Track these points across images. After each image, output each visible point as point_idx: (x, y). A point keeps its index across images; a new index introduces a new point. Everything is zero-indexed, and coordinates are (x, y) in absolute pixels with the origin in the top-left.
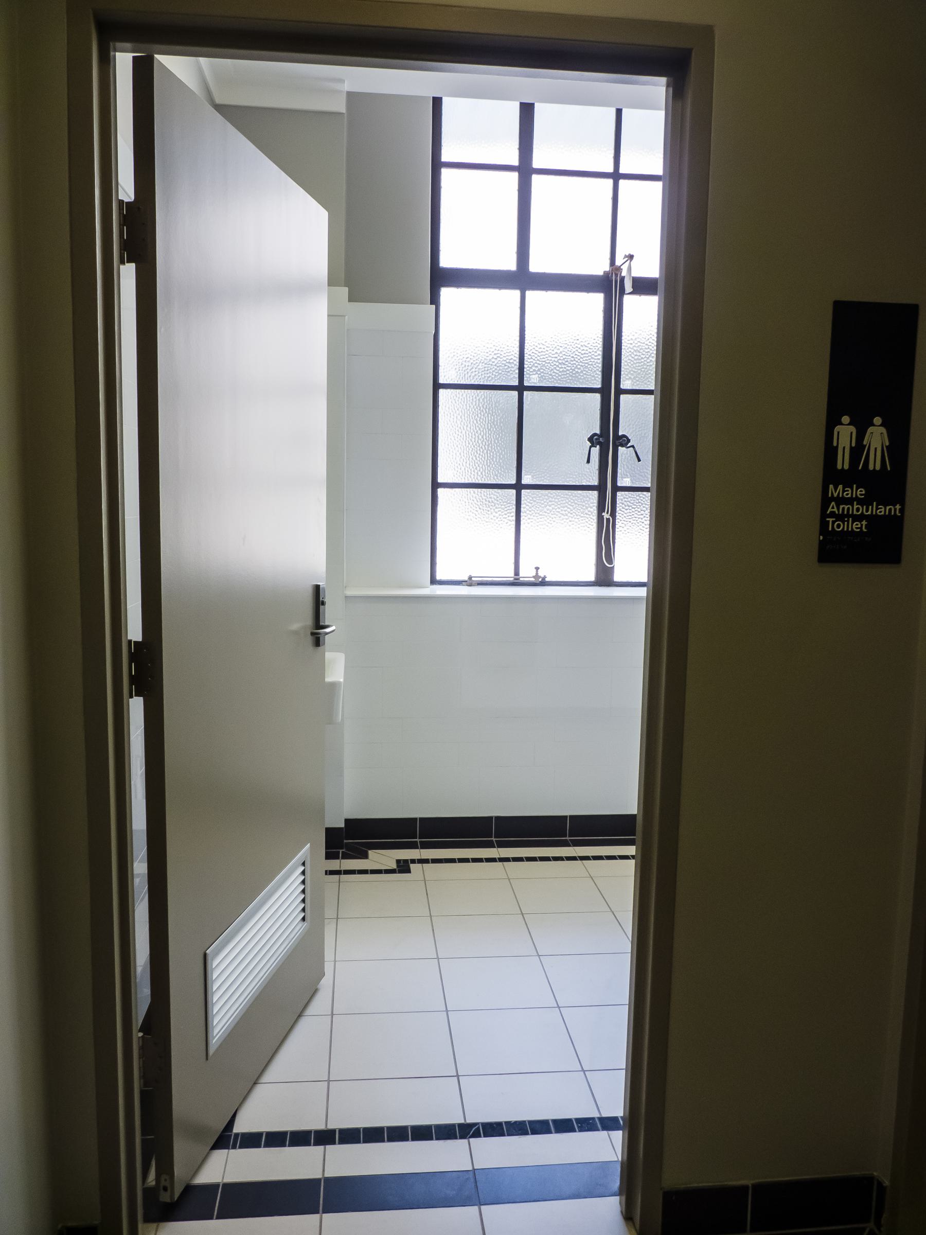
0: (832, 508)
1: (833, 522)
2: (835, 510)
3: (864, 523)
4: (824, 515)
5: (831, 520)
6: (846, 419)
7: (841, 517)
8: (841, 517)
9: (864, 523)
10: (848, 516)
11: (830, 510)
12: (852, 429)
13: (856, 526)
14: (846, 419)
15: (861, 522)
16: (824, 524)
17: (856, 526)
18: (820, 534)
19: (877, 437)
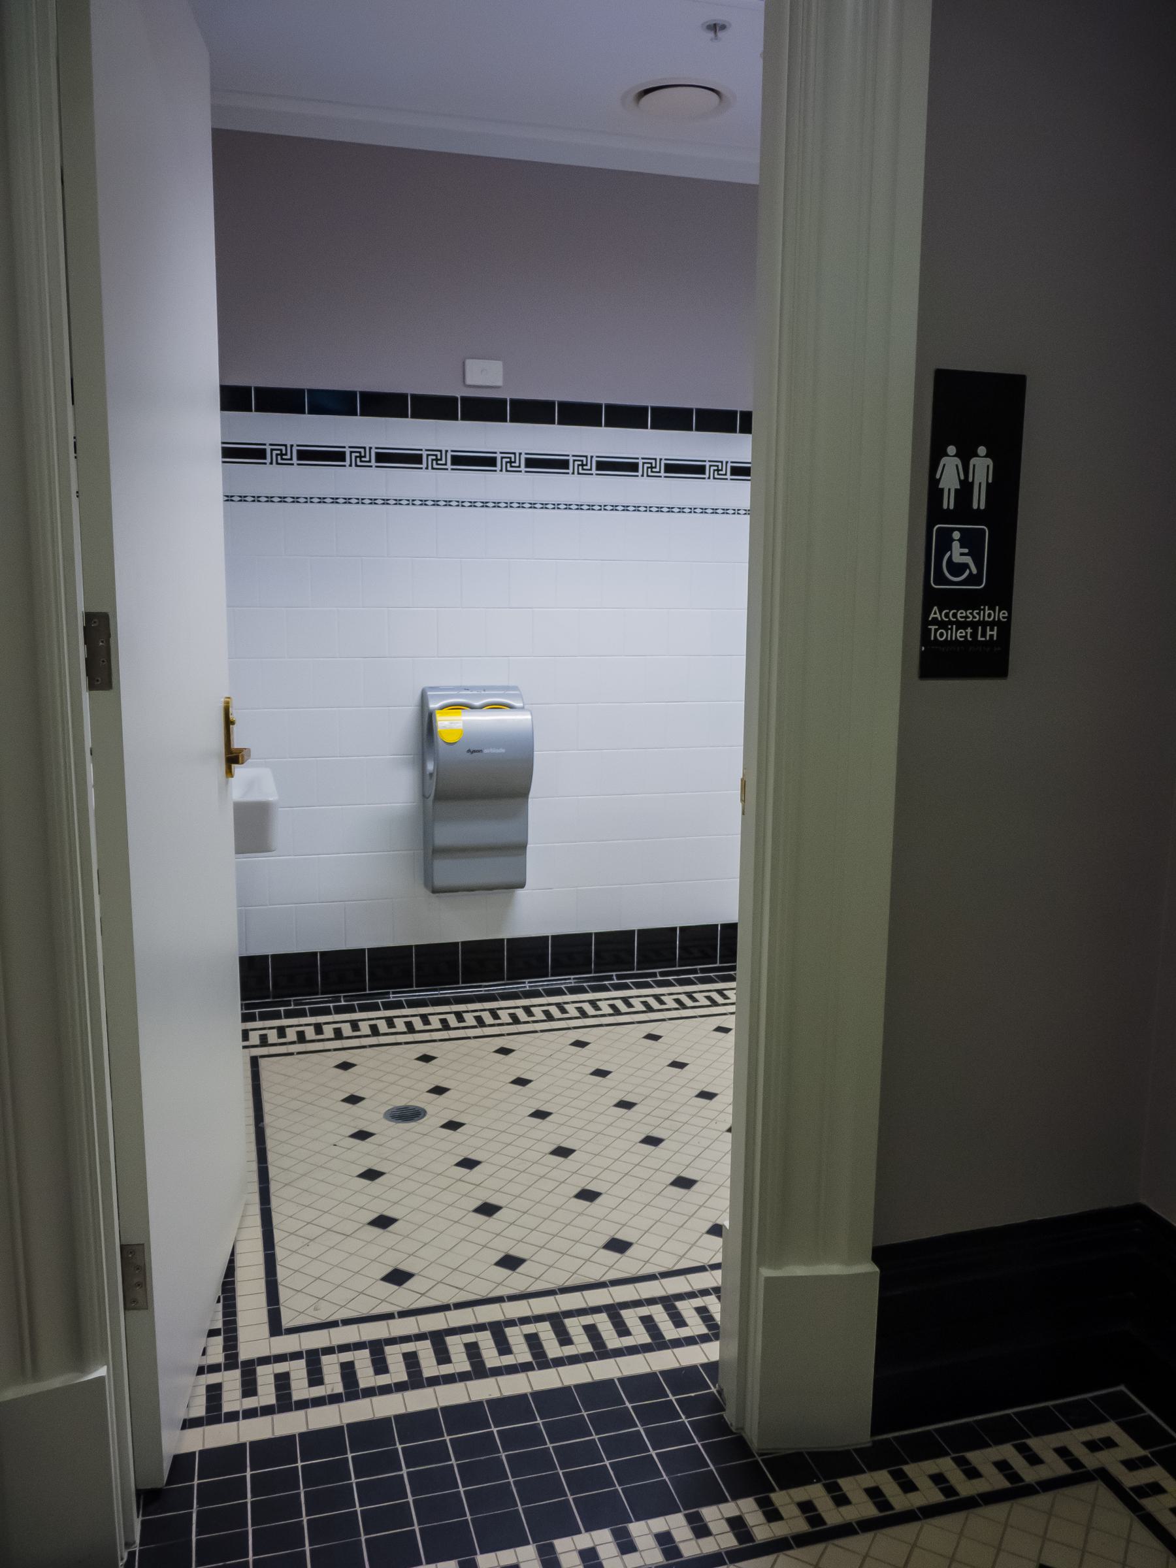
0: (935, 614)
1: (936, 630)
2: (938, 615)
3: (969, 630)
4: (926, 622)
5: (933, 628)
6: (952, 450)
7: (943, 625)
8: (943, 625)
9: (969, 630)
10: (950, 622)
11: (932, 615)
12: (957, 461)
13: (960, 635)
14: (952, 450)
15: (965, 629)
16: (925, 633)
17: (960, 635)
18: (922, 645)
19: (982, 467)
